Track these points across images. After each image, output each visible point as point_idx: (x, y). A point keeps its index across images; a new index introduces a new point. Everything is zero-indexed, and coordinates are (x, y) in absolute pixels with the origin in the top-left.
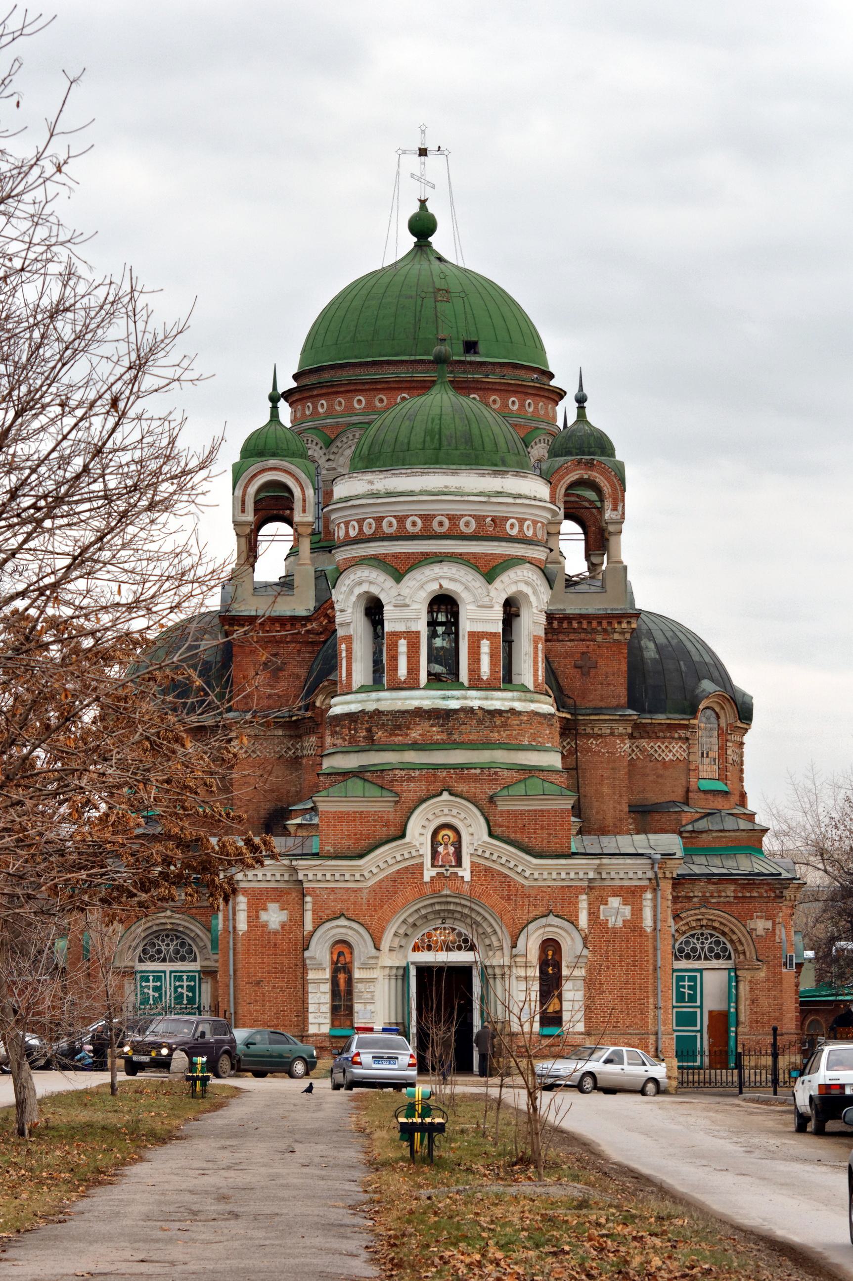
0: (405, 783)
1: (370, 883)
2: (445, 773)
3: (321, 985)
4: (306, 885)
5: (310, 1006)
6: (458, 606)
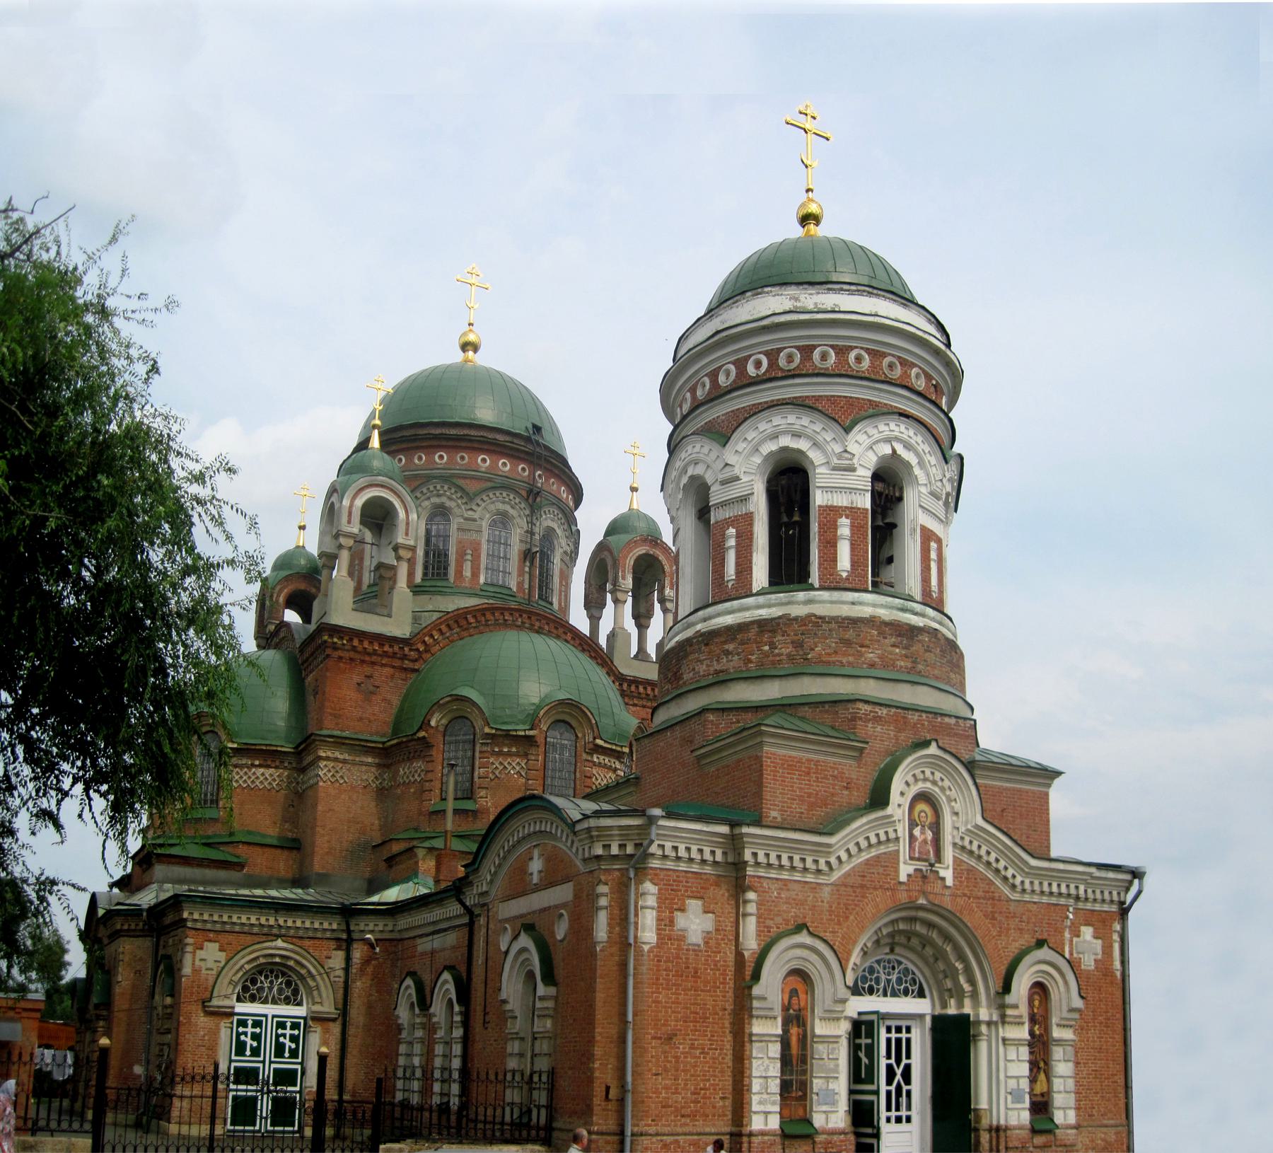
0: (870, 725)
1: (836, 876)
2: (916, 718)
3: (770, 1045)
4: (750, 871)
5: (754, 1081)
6: (901, 489)
